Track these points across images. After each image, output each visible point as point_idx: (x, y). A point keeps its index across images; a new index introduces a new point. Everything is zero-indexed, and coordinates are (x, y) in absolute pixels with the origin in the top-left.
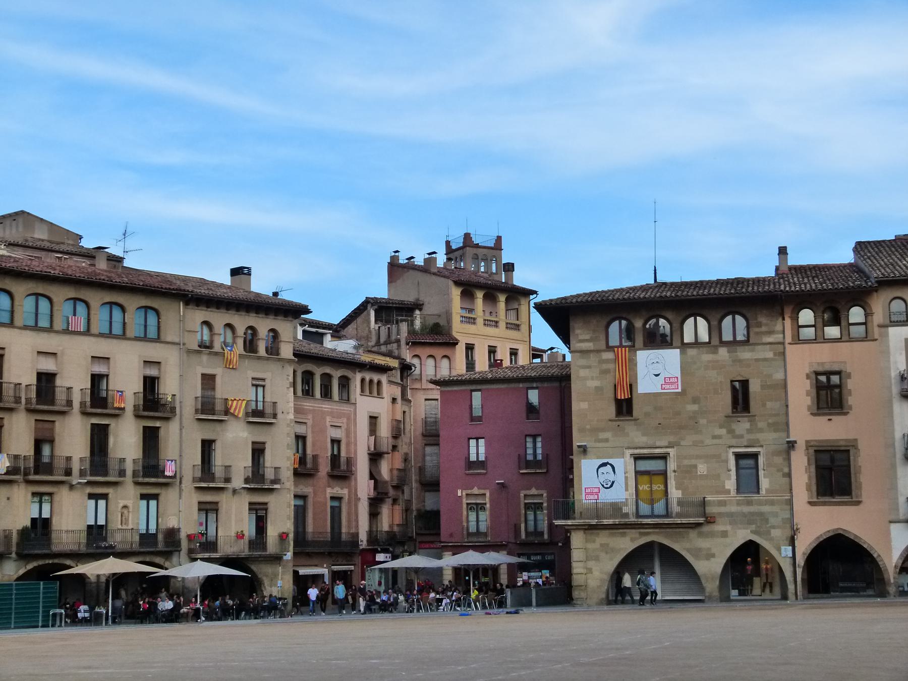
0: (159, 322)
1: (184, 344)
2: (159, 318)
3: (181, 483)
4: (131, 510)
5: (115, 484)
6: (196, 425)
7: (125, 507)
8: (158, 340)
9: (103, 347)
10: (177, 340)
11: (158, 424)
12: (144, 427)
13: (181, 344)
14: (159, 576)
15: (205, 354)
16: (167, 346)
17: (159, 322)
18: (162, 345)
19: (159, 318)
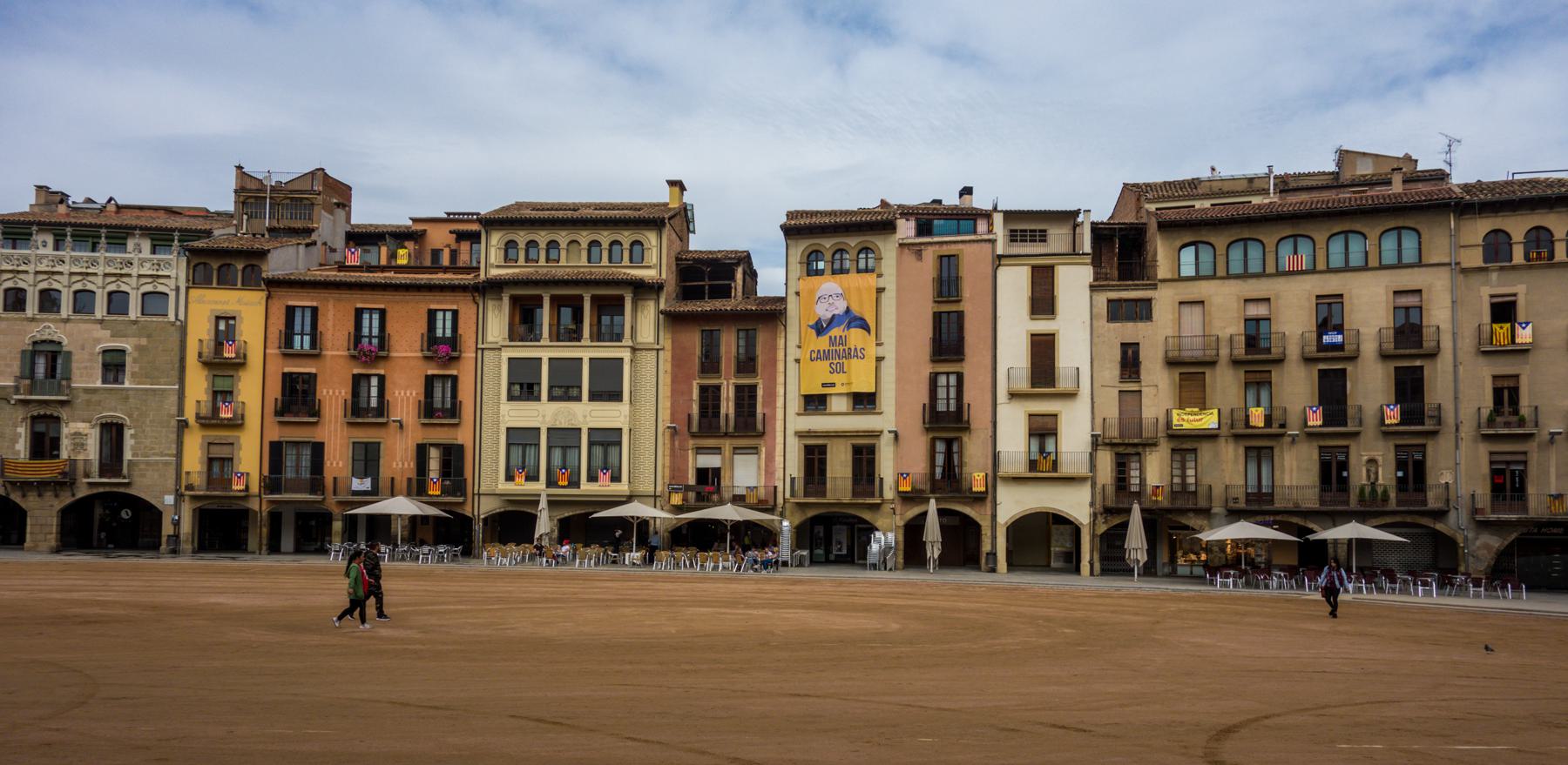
0: (1420, 243)
1: (1458, 264)
2: (1420, 238)
3: (1457, 430)
4: (1380, 462)
5: (1356, 435)
6: (1482, 360)
7: (1372, 461)
8: (1419, 264)
9: (1331, 284)
10: (1446, 260)
11: (1418, 363)
12: (1396, 368)
13: (1453, 264)
14: (1286, 533)
15: (1494, 271)
16: (1430, 269)
17: (1420, 243)
18: (1424, 269)
19: (1420, 238)
